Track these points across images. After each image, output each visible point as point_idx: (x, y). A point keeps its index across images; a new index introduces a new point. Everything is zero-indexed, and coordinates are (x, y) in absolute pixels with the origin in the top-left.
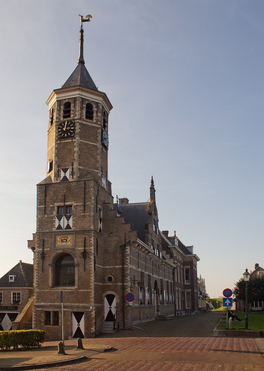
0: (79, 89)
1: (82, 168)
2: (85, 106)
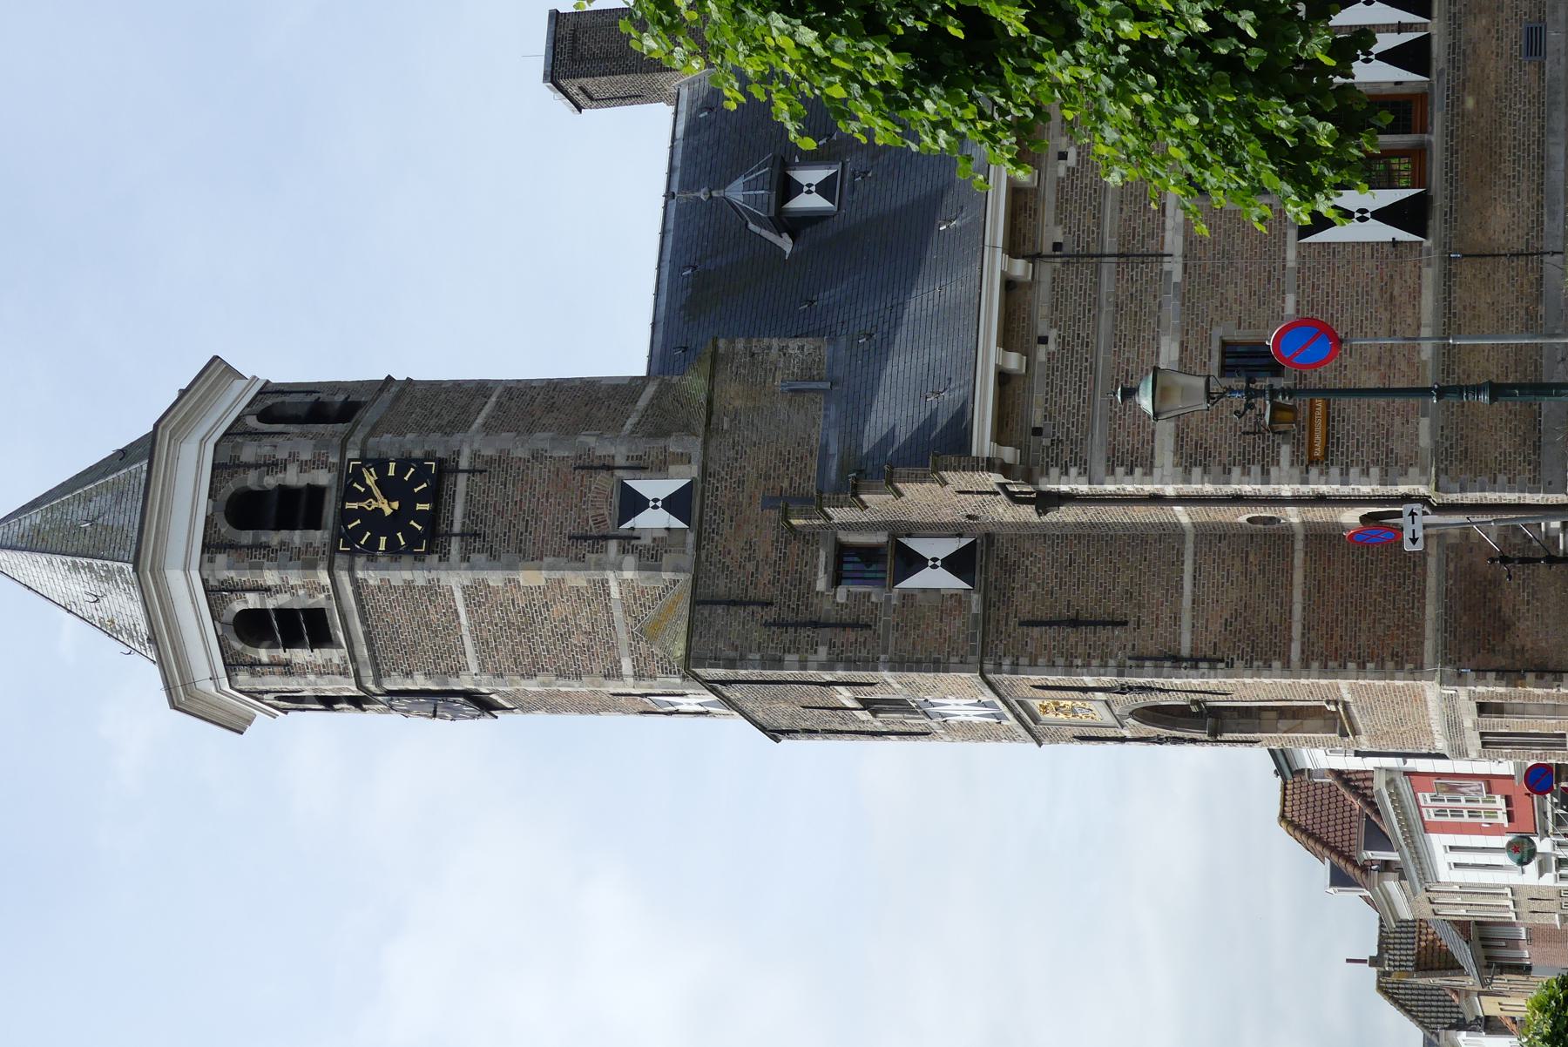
0: (158, 571)
1: (627, 666)
2: (263, 654)
